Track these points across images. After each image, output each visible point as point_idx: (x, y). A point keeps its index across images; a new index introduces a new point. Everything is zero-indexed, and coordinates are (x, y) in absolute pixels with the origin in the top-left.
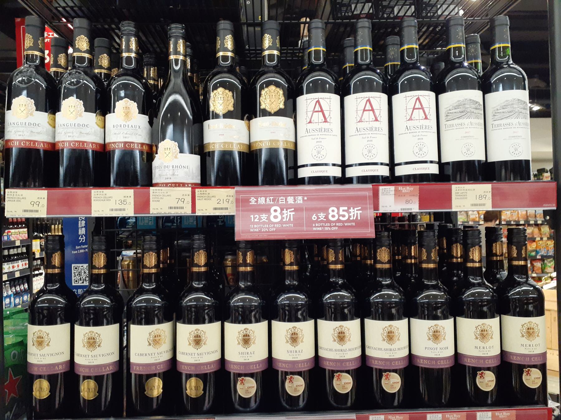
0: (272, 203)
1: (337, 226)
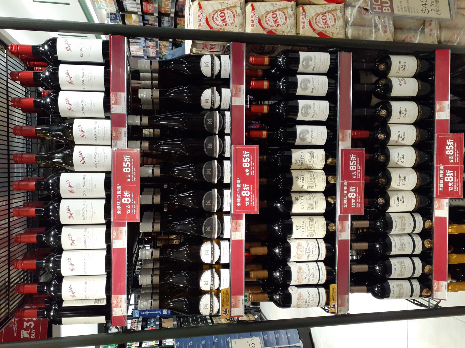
0: (120, 203)
1: (134, 168)
